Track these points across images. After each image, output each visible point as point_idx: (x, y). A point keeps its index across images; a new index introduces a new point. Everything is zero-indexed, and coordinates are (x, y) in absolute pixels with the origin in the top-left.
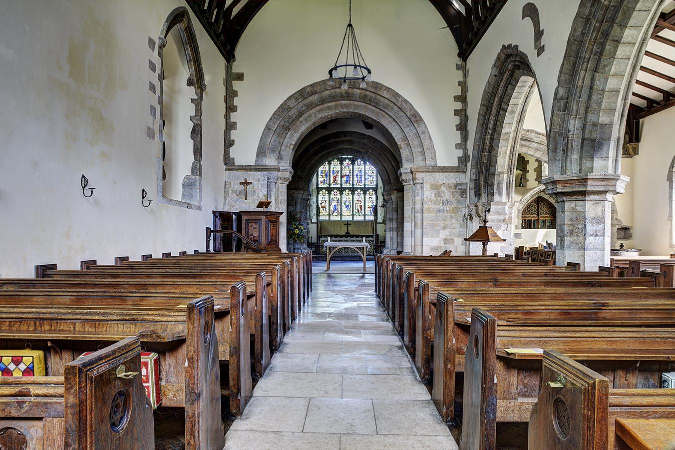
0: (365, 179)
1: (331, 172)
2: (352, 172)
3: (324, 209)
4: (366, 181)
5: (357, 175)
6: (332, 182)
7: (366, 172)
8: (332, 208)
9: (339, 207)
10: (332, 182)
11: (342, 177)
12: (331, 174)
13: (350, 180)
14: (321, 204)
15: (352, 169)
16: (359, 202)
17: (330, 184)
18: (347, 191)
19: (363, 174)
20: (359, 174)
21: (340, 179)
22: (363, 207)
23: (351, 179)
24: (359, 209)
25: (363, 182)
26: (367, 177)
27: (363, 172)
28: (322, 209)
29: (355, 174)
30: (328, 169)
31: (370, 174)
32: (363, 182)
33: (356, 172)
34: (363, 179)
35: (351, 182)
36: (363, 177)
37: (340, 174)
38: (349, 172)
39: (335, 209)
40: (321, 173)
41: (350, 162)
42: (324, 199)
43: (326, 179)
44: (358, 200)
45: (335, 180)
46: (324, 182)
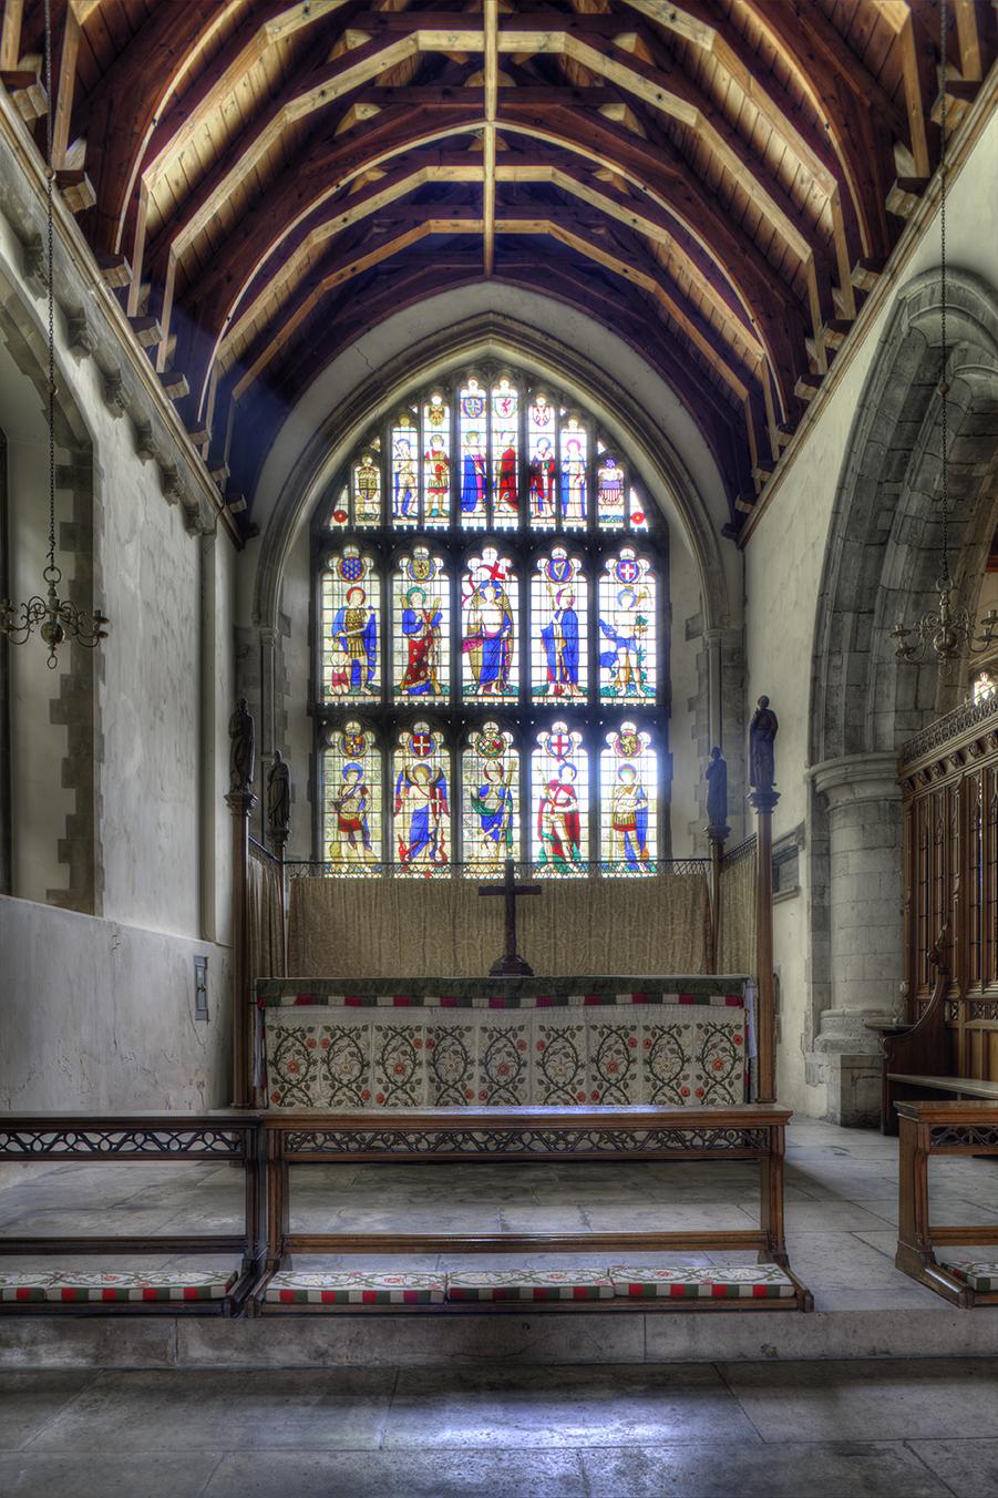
0: (596, 661)
1: (398, 616)
2: (516, 617)
3: (358, 835)
4: (604, 674)
5: (547, 637)
6: (399, 674)
7: (603, 616)
8: (402, 826)
9: (446, 821)
10: (399, 674)
11: (458, 645)
12: (398, 631)
13: (506, 668)
14: (337, 805)
15: (515, 603)
16: (563, 795)
17: (387, 690)
18: (491, 727)
19: (583, 631)
20: (558, 631)
21: (446, 659)
22: (584, 820)
23: (515, 660)
24: (562, 834)
25: (583, 674)
26: (606, 646)
27: (583, 618)
28: (344, 836)
29: (536, 631)
30: (376, 602)
31: (624, 633)
32: (583, 674)
33: (540, 621)
34: (583, 660)
35: (514, 676)
36: (583, 646)
37: (445, 630)
38: (497, 617)
39: (422, 837)
40: (338, 624)
41: (505, 563)
42: (353, 778)
43: (363, 660)
44: (553, 785)
45: (418, 667)
46: (356, 676)
